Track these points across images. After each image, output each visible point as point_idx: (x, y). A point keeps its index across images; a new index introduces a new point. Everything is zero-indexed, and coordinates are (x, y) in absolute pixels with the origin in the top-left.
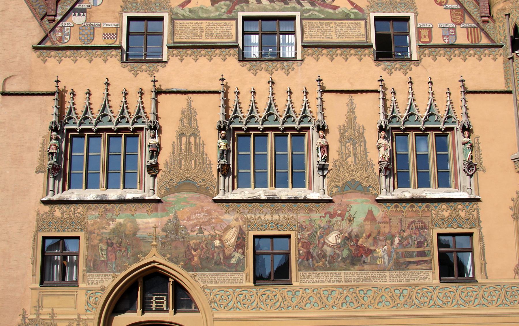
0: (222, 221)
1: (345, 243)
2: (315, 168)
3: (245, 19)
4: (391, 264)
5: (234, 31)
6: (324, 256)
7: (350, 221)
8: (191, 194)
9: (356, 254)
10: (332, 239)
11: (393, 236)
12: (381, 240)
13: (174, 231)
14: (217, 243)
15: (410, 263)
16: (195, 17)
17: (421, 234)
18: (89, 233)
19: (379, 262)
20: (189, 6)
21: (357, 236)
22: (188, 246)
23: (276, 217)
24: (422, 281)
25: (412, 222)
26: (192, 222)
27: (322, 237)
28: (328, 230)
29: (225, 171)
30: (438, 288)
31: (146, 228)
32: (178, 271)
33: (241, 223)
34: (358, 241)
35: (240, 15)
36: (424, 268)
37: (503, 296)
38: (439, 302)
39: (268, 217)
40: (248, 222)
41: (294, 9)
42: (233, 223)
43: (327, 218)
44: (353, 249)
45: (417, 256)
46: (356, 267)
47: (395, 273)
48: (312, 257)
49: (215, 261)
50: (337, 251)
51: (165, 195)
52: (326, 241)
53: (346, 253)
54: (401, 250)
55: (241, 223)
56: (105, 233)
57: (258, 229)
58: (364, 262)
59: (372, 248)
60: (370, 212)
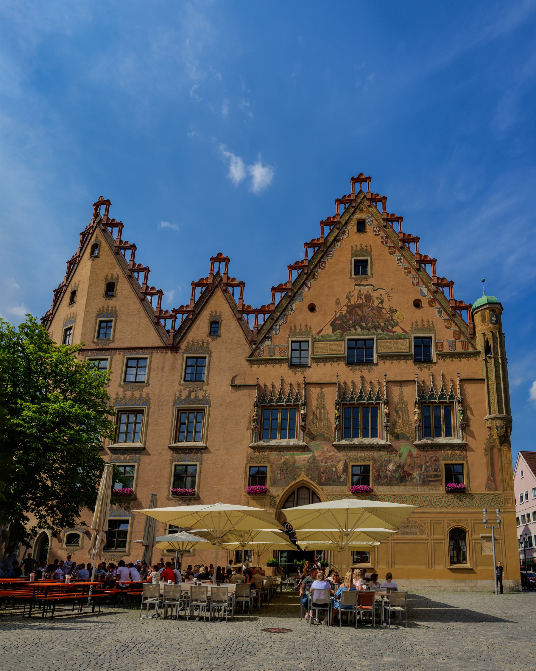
0: (336, 457)
2: (383, 426)
3: (349, 340)
4: (421, 482)
5: (343, 348)
6: (387, 477)
7: (400, 456)
8: (321, 442)
9: (403, 477)
10: (391, 467)
11: (422, 466)
15: (430, 481)
16: (324, 340)
17: (436, 465)
19: (414, 480)
20: (321, 334)
21: (403, 465)
22: (320, 471)
23: (363, 454)
24: (437, 492)
25: (432, 457)
26: (321, 458)
27: (386, 466)
28: (389, 462)
29: (337, 429)
32: (314, 484)
33: (345, 458)
34: (404, 468)
35: (347, 338)
38: (445, 504)
40: (349, 457)
41: (373, 334)
42: (342, 458)
43: (388, 455)
44: (401, 473)
46: (403, 483)
47: (423, 487)
48: (381, 477)
53: (398, 475)
54: (426, 474)
55: (345, 458)
57: (354, 461)
59: (411, 472)
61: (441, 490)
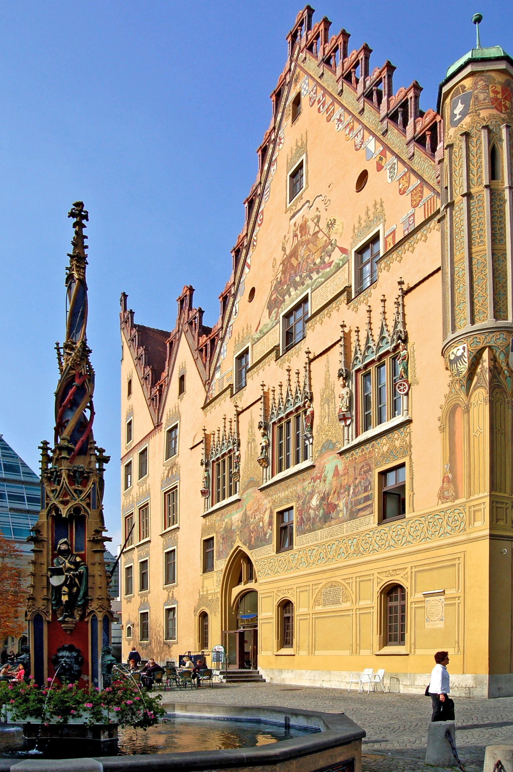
1: (321, 503)
4: (348, 515)
7: (325, 481)
9: (328, 513)
10: (315, 502)
11: (350, 486)
12: (342, 493)
13: (245, 519)
14: (261, 523)
15: (359, 510)
18: (217, 533)
20: (259, 328)
23: (287, 493)
24: (367, 528)
27: (309, 502)
28: (312, 494)
30: (376, 532)
31: (235, 522)
36: (368, 513)
37: (426, 529)
39: (283, 495)
44: (325, 507)
45: (364, 502)
48: (304, 522)
49: (261, 541)
50: (316, 512)
51: (244, 492)
52: (311, 505)
53: (321, 511)
56: (221, 531)
58: (332, 518)
59: (336, 503)
60: (336, 467)
61: (371, 522)
